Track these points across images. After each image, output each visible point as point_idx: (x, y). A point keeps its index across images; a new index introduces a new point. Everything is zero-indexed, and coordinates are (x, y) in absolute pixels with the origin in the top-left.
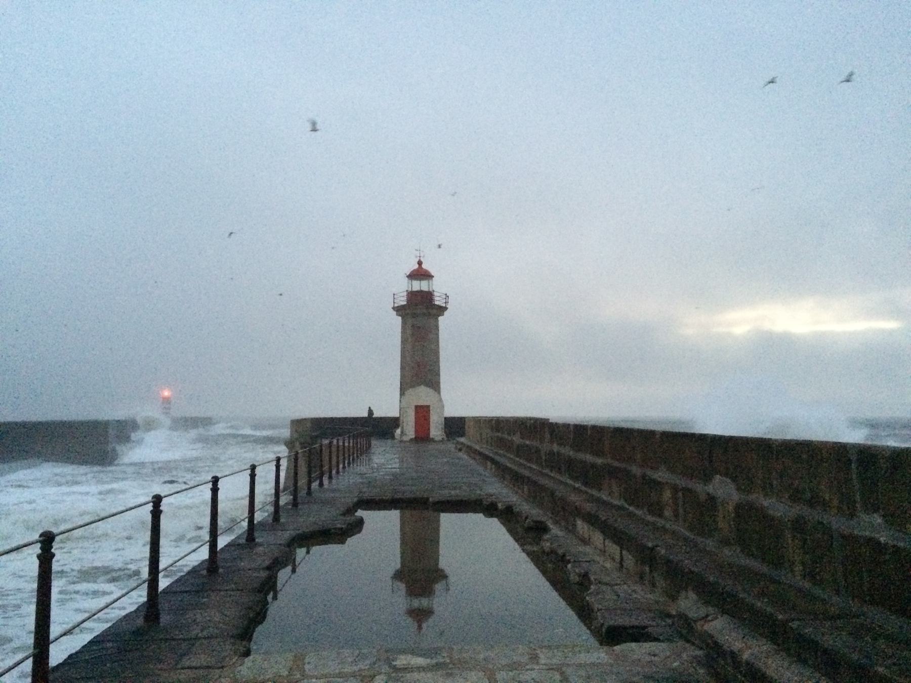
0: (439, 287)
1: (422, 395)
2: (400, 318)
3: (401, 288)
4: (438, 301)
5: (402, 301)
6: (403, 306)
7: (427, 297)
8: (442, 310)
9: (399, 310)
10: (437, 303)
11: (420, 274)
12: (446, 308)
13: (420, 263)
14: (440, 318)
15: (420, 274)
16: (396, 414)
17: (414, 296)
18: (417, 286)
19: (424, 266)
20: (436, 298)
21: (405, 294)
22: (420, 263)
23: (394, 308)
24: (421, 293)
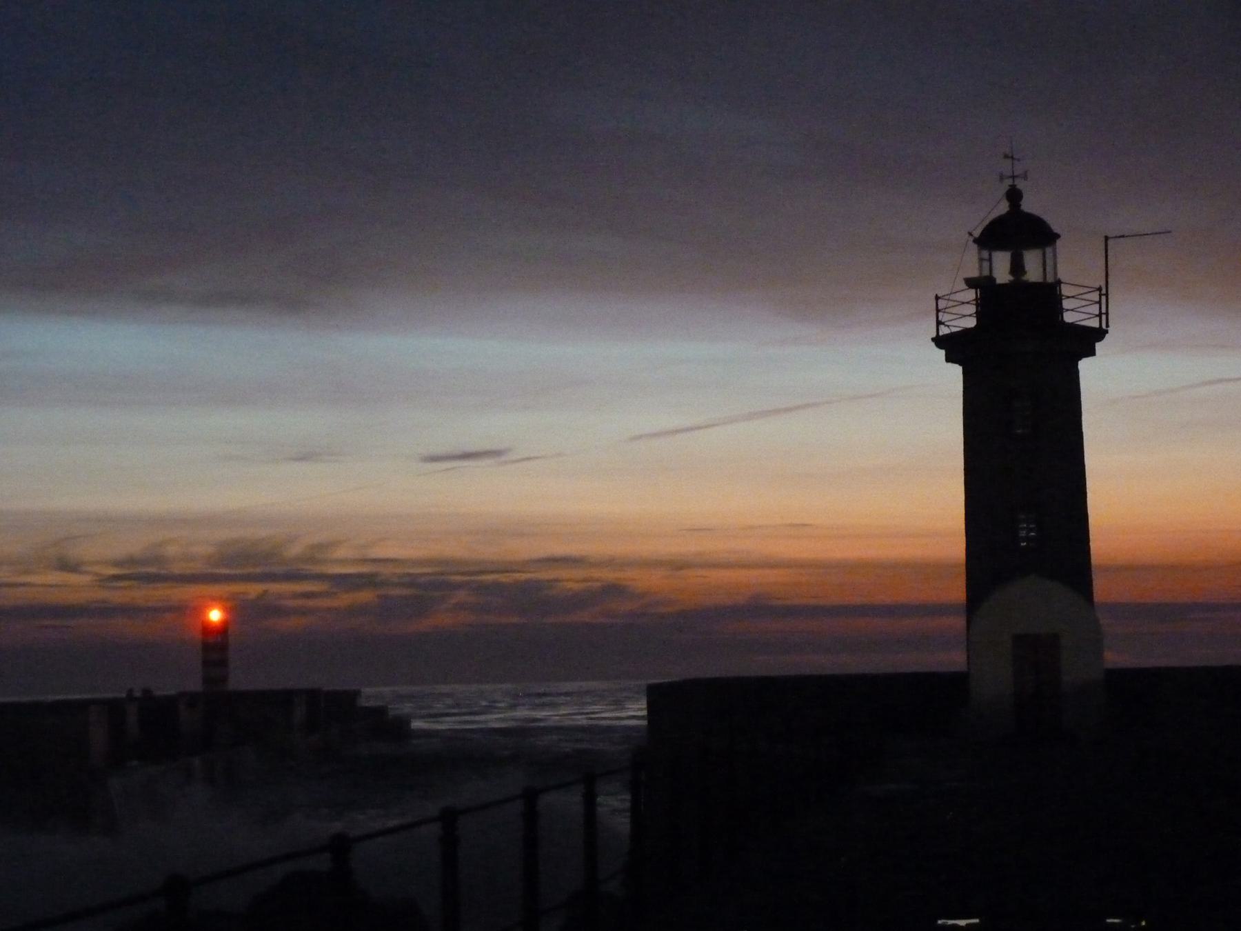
1: (1032, 602)
2: (956, 371)
4: (1076, 313)
6: (966, 332)
8: (1086, 340)
10: (1069, 318)
11: (1017, 230)
12: (1100, 334)
13: (1014, 196)
14: (1084, 365)
16: (954, 660)
20: (1066, 304)
21: (971, 295)
22: (1014, 196)
23: (939, 341)
24: (1019, 286)
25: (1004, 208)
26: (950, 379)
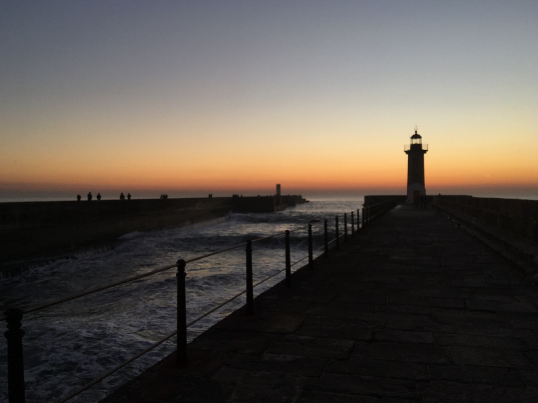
0: (425, 142)
3: (407, 143)
4: (424, 148)
5: (408, 148)
7: (420, 146)
8: (425, 151)
9: (407, 152)
11: (416, 136)
13: (416, 132)
15: (416, 136)
16: (405, 194)
17: (413, 146)
18: (416, 141)
19: (418, 133)
22: (416, 132)
23: (405, 151)
25: (414, 133)
26: (406, 156)
